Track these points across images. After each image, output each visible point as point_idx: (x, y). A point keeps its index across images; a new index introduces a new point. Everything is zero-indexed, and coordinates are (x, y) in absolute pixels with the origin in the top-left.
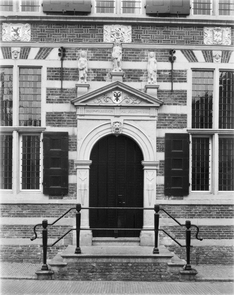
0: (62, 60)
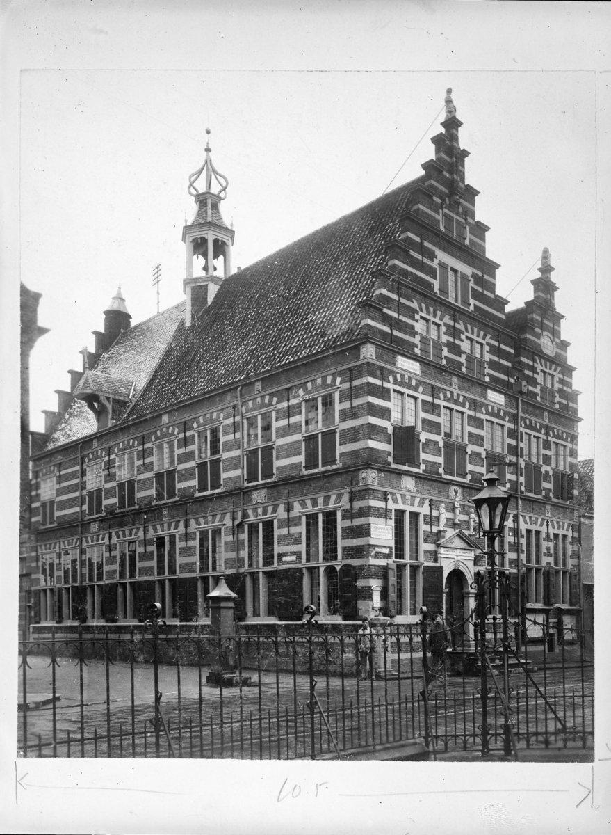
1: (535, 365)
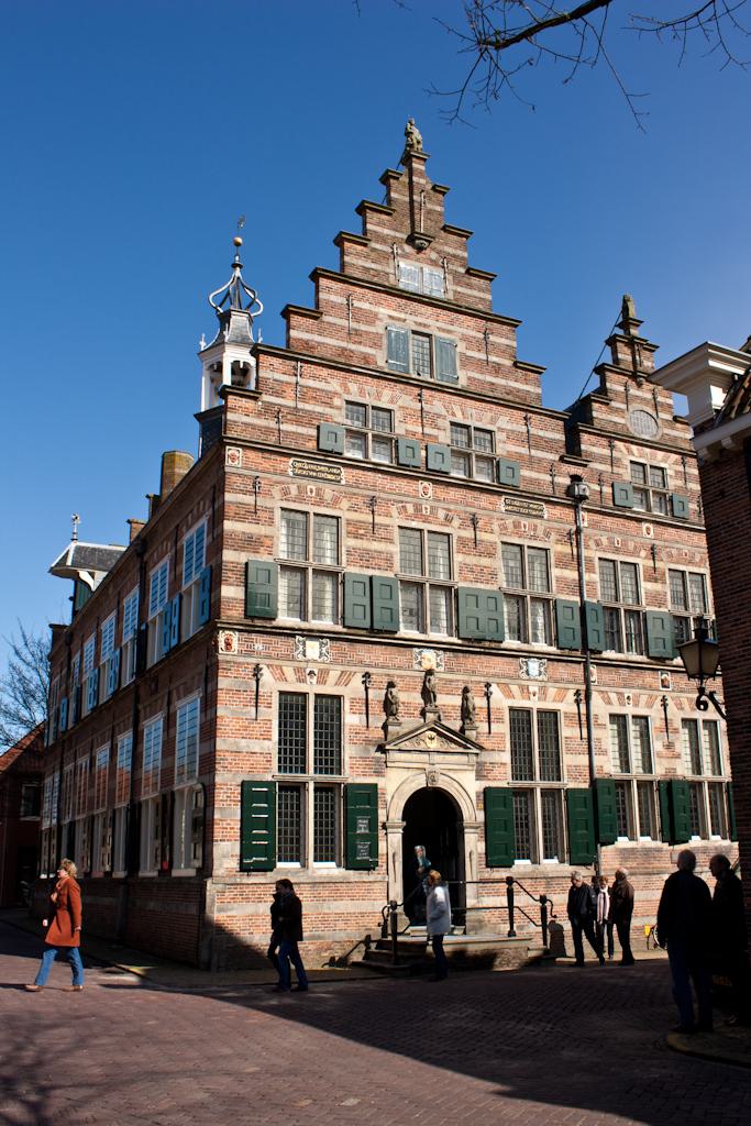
0: (366, 689)
1: (615, 454)
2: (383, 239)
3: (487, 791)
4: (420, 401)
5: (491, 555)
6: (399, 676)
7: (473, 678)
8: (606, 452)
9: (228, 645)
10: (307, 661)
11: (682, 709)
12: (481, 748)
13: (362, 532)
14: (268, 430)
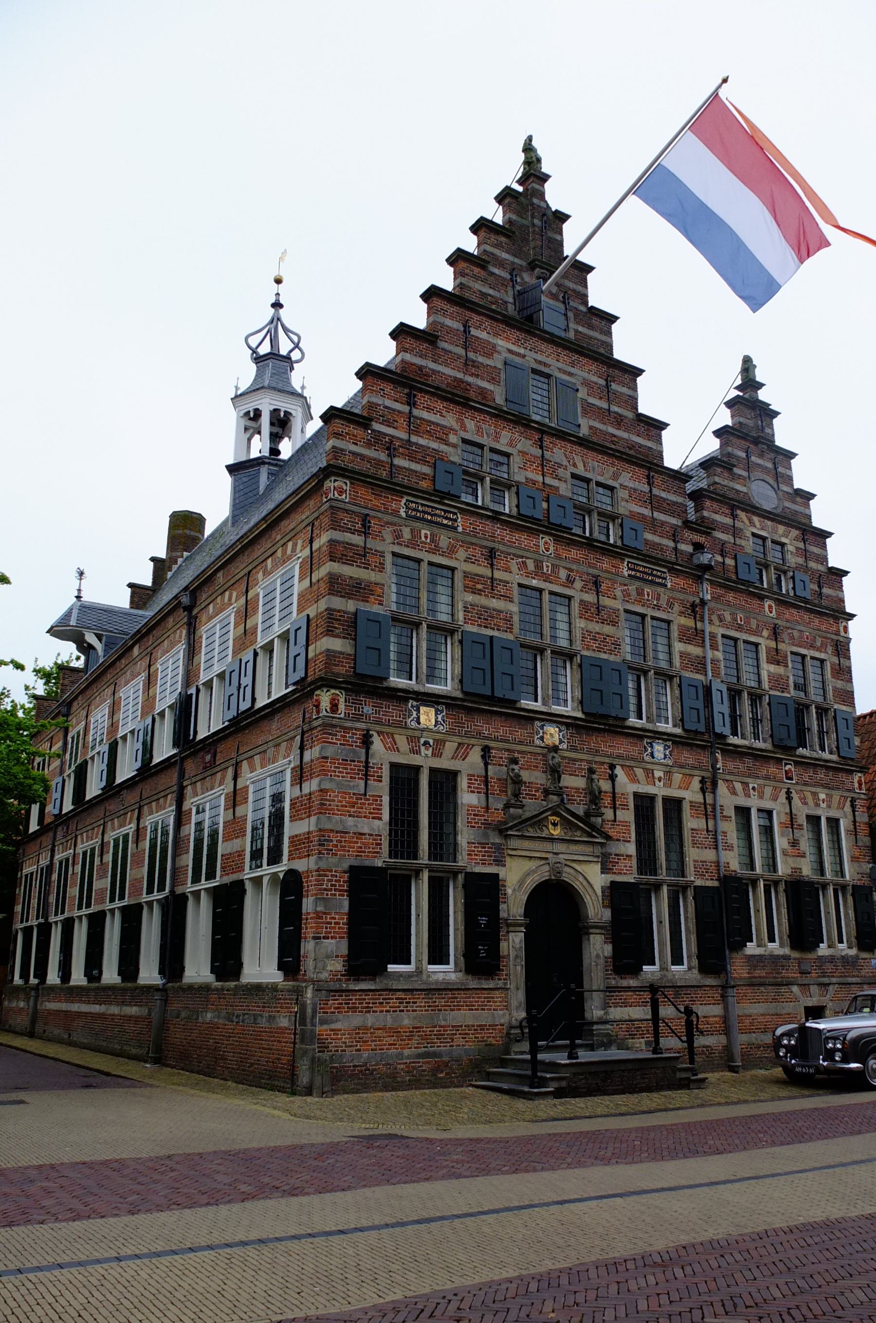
0: (486, 764)
1: (738, 524)
2: (501, 264)
3: (614, 886)
4: (541, 447)
5: (614, 623)
6: (519, 752)
7: (597, 759)
8: (728, 521)
9: (334, 707)
10: (423, 730)
11: (806, 804)
12: (608, 838)
13: (479, 587)
14: (379, 463)
